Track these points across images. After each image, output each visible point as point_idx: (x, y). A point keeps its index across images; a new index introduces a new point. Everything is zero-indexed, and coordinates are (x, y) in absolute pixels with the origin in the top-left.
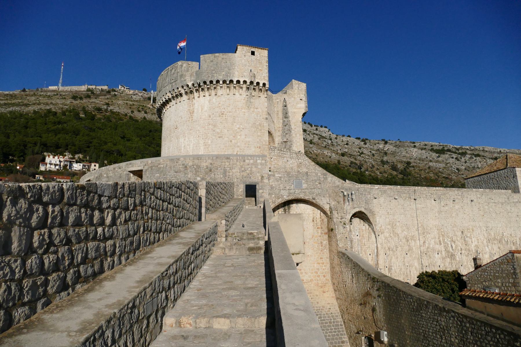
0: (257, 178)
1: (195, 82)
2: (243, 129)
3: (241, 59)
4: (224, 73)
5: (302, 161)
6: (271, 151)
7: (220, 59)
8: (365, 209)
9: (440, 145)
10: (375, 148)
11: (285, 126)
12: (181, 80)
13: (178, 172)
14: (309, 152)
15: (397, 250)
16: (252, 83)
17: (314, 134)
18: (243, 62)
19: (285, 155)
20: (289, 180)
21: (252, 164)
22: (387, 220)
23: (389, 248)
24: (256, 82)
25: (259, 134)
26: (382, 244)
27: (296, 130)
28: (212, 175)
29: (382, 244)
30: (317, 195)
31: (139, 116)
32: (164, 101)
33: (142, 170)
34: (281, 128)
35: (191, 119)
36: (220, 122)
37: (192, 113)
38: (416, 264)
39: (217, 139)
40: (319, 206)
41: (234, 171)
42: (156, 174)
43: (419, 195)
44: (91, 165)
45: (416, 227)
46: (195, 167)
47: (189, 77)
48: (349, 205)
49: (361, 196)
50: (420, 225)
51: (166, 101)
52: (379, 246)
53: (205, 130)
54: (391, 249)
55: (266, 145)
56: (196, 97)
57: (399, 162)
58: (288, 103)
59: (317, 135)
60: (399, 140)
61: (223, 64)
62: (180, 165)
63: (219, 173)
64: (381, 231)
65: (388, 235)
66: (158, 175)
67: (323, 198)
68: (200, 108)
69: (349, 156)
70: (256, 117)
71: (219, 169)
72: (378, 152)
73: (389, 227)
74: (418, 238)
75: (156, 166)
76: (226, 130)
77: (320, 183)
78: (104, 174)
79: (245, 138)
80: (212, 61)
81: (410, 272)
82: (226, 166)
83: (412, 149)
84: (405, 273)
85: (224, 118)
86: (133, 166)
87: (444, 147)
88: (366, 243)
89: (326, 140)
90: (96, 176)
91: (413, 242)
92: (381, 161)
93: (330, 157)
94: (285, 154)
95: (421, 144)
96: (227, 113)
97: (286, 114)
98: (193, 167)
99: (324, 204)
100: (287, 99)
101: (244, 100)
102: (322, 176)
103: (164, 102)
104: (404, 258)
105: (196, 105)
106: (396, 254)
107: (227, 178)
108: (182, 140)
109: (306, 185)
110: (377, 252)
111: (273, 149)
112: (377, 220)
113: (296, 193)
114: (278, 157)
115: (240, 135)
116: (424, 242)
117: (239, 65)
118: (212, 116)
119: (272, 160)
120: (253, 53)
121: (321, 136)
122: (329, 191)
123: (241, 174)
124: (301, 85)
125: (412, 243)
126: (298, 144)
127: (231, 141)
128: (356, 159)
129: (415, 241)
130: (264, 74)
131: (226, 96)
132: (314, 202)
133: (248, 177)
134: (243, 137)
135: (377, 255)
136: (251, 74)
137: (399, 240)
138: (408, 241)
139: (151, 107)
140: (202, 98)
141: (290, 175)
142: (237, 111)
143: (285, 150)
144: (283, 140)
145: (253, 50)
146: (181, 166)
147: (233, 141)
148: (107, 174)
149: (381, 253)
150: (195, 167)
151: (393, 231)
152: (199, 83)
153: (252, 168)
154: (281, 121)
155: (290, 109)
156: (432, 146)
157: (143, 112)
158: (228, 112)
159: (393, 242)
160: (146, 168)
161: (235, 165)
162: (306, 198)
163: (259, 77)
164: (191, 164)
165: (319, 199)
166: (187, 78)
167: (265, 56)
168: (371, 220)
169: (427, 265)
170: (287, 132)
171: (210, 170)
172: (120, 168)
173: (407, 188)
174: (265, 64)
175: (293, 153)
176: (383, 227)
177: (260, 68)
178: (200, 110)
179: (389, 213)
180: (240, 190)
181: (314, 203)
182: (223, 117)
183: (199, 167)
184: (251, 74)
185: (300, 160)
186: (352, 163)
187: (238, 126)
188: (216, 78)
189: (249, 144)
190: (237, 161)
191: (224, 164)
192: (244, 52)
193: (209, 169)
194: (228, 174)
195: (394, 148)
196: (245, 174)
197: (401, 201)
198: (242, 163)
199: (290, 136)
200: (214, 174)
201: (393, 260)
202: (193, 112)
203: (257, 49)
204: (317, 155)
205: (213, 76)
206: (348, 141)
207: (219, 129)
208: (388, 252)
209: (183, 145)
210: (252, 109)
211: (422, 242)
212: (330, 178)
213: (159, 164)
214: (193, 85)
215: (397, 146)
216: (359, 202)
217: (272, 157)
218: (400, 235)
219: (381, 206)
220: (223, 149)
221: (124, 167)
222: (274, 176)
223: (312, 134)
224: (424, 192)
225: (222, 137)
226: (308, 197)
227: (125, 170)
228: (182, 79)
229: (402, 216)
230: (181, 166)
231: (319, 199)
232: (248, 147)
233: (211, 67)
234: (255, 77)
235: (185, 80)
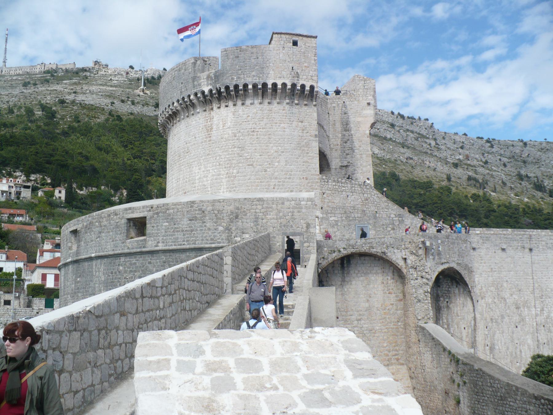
0: (300, 227)
1: (213, 87)
2: (283, 152)
3: (278, 52)
4: (254, 73)
5: (369, 196)
6: (323, 183)
8: (458, 264)
10: (508, 154)
11: (346, 142)
12: (194, 84)
13: (193, 220)
14: (399, 162)
15: (502, 322)
16: (294, 85)
17: (408, 130)
18: (281, 56)
19: (343, 188)
20: (349, 225)
21: (294, 208)
22: (490, 279)
23: (492, 319)
24: (300, 84)
25: (305, 159)
26: (482, 314)
27: (361, 148)
28: (240, 223)
29: (482, 314)
30: (388, 247)
31: (124, 109)
32: (170, 113)
33: (146, 217)
34: (339, 147)
35: (208, 139)
36: (250, 144)
37: (209, 129)
38: (530, 341)
39: (245, 168)
40: (391, 262)
41: (269, 217)
42: (165, 222)
43: (536, 243)
44: (54, 191)
45: (531, 288)
46: (216, 212)
47: (206, 80)
48: (434, 259)
49: (451, 246)
50: (536, 285)
51: (174, 113)
52: (478, 316)
53: (228, 155)
54: (494, 321)
55: (316, 175)
56: (215, 108)
58: (348, 107)
59: (412, 132)
60: (546, 139)
61: (253, 60)
62: (196, 210)
63: (248, 221)
64: (480, 295)
65: (490, 300)
66: (167, 224)
67: (396, 251)
68: (221, 123)
69: (466, 167)
70: (301, 134)
71: (248, 215)
72: (512, 160)
73: (492, 288)
74: (533, 304)
75: (163, 213)
77: (393, 229)
78: (96, 222)
79: (286, 165)
81: (521, 351)
82: (257, 211)
84: (514, 353)
85: (255, 137)
86: (133, 213)
88: (459, 312)
89: (428, 141)
90: (85, 224)
91: (526, 309)
92: (517, 175)
93: (435, 170)
94: (344, 187)
96: (259, 130)
97: (347, 124)
98: (212, 212)
99: (398, 259)
100: (347, 103)
101: (284, 110)
102: (397, 219)
103: (170, 115)
104: (513, 333)
105: (215, 119)
106: (502, 328)
107: (259, 227)
108: (195, 170)
109: (374, 232)
110: (475, 325)
111: (326, 181)
112: (476, 279)
113: (358, 244)
114: (333, 192)
115: (279, 162)
116: (542, 310)
117: (275, 61)
118: (237, 135)
119: (325, 196)
120: (295, 43)
121: (419, 134)
122: (405, 240)
123: (278, 221)
124: (368, 82)
125: (526, 312)
126: (364, 169)
127: (266, 171)
128: (476, 172)
129: (528, 307)
130: (311, 72)
131: (258, 106)
132: (384, 257)
133: (288, 226)
134: (283, 163)
135: (475, 330)
136: (292, 73)
137: (507, 307)
138: (518, 308)
139: (141, 93)
140: (223, 108)
141: (351, 218)
142: (274, 127)
143: (344, 181)
144: (342, 163)
145: (295, 38)
146: (197, 212)
147: (268, 170)
149: (481, 325)
150: (216, 212)
151: (498, 295)
152: (218, 88)
153: (293, 212)
154: (340, 135)
155: (353, 119)
157: (129, 103)
158: (260, 128)
159: (497, 310)
161: (271, 209)
162: (373, 251)
163: (305, 77)
164: (210, 208)
165: (390, 252)
166: (202, 80)
167: (312, 47)
168: (467, 279)
169: (545, 341)
170: (347, 152)
171: (237, 217)
172: (116, 215)
173: (523, 233)
174: (313, 58)
175: (355, 184)
176: (484, 289)
177: (306, 64)
178: (221, 126)
179: (494, 270)
180: (278, 244)
181: (384, 258)
182: (253, 135)
184: (292, 73)
185: (366, 195)
186: (470, 178)
187: (275, 148)
188: (243, 80)
189: (291, 175)
190: (273, 203)
191: (254, 207)
192: (282, 42)
193: (234, 215)
194: (260, 220)
195: (539, 153)
196: (284, 221)
197: (510, 251)
198: (280, 206)
199: (352, 157)
200: (242, 222)
201: (496, 337)
202: (212, 128)
203: (301, 38)
204: (412, 167)
205: (239, 78)
206: (463, 142)
207: (248, 153)
208: (490, 324)
210: (295, 123)
211: (539, 310)
212: (409, 221)
213: (168, 209)
214: (211, 91)
215: (542, 149)
216: (449, 254)
217: (324, 191)
218: (508, 301)
219: (482, 260)
220: (255, 182)
221: (121, 213)
222: (327, 219)
223: (404, 131)
224: (544, 239)
225: (252, 165)
226: (375, 250)
227: (123, 217)
228: (196, 83)
229: (512, 273)
230: (197, 212)
231: (390, 252)
232: (289, 178)
233: (236, 65)
234: (298, 77)
235: (200, 85)
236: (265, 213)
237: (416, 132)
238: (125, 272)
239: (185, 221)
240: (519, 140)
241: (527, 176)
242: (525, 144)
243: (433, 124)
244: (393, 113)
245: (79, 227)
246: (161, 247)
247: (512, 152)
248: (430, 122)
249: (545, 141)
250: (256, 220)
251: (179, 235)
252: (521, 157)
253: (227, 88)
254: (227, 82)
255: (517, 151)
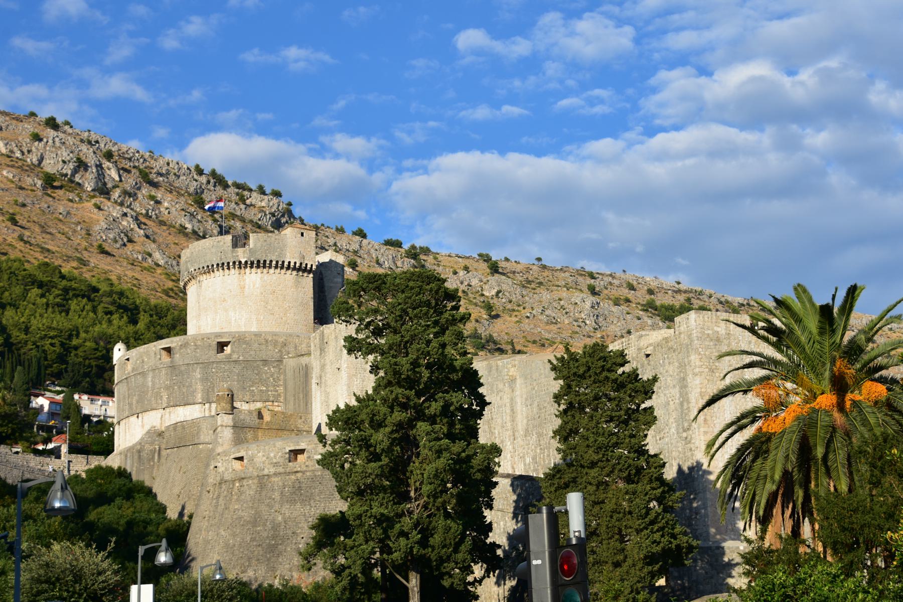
7: (273, 239)
9: (679, 291)
16: (301, 264)
28: (287, 348)
37: (242, 288)
57: (534, 342)
60: (539, 259)
76: (277, 308)
80: (265, 241)
83: (577, 297)
87: (688, 300)
90: (180, 344)
95: (616, 282)
100: (323, 272)
120: (302, 234)
140: (253, 275)
148: (194, 343)
156: (651, 292)
160: (234, 340)
183: (276, 341)
206: (355, 252)
209: (233, 319)
214: (246, 262)
215: (529, 282)
236: (301, 344)
237: (251, 221)
238: (217, 372)
239: (256, 345)
240: (480, 255)
241: (490, 339)
242: (495, 269)
243: (290, 204)
244: (200, 172)
245: (172, 345)
246: (241, 358)
247: (462, 283)
248: (285, 199)
249: (536, 263)
250: (296, 347)
251: (252, 353)
252: (483, 295)
253: (259, 261)
254: (259, 258)
255: (475, 282)
